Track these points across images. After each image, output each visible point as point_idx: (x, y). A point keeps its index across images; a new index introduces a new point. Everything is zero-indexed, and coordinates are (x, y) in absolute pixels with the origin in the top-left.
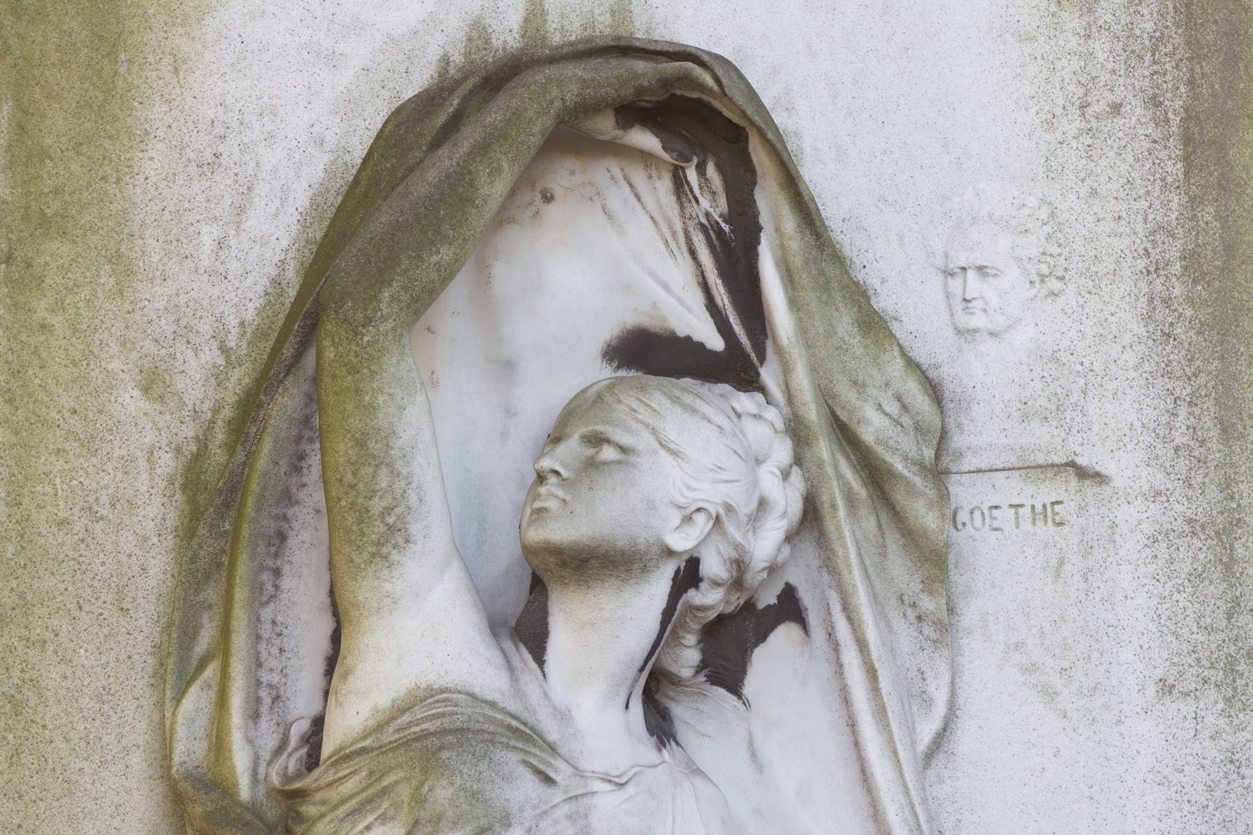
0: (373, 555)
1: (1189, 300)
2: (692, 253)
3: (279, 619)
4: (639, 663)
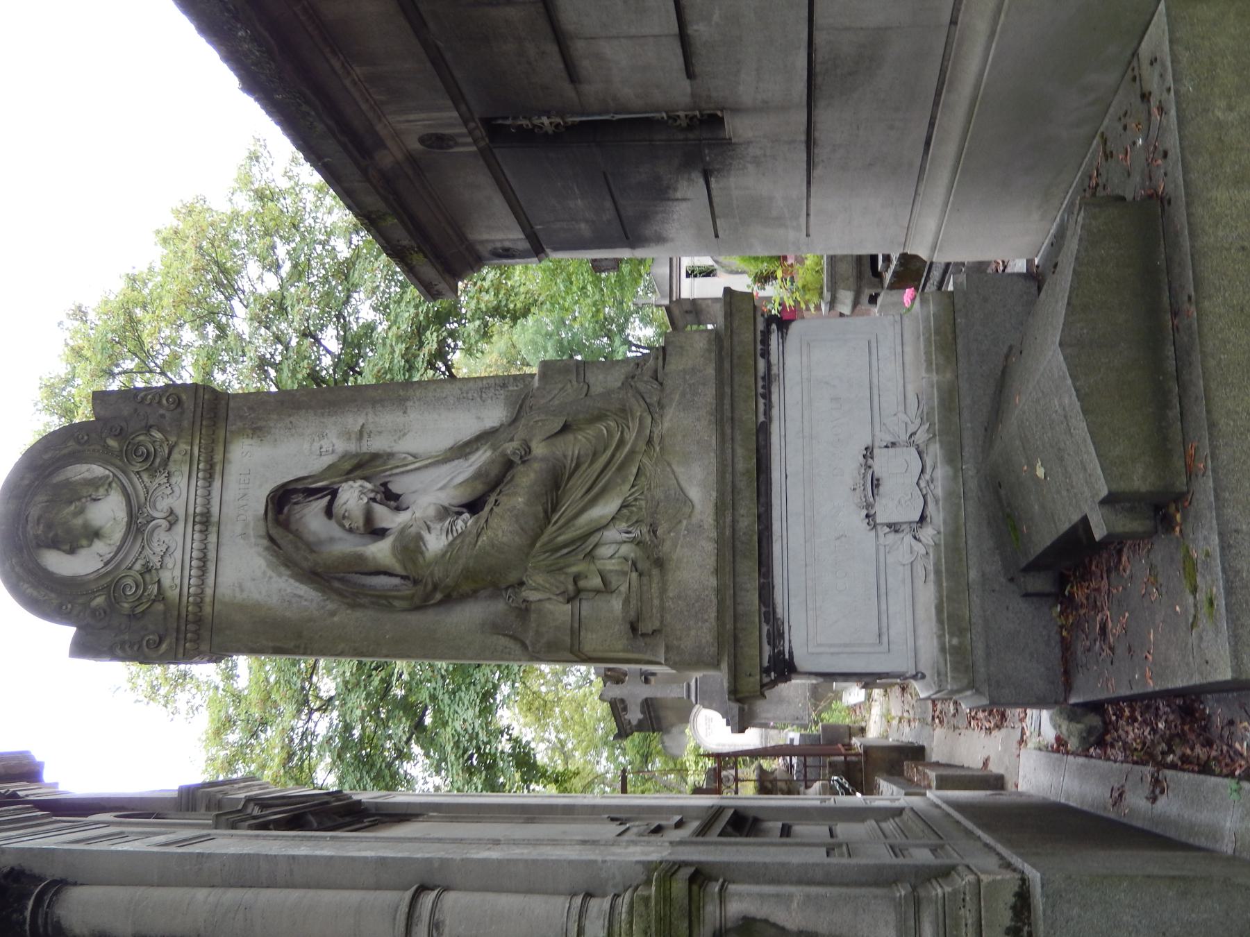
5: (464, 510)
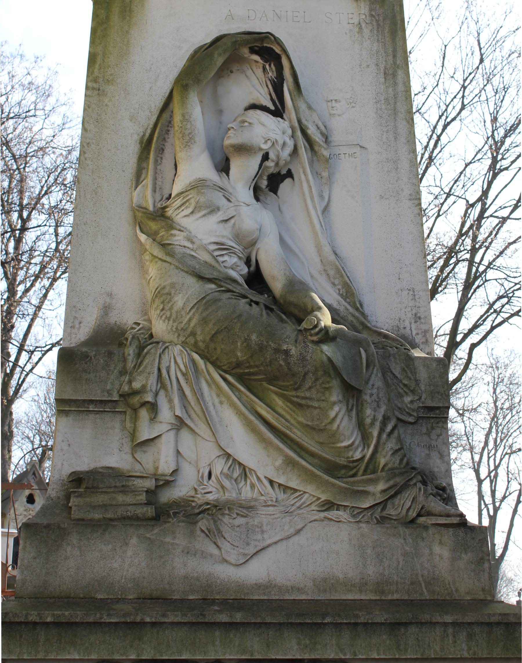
0: (186, 145)
1: (386, 109)
2: (267, 86)
3: (162, 169)
4: (253, 178)
5: (252, 268)
